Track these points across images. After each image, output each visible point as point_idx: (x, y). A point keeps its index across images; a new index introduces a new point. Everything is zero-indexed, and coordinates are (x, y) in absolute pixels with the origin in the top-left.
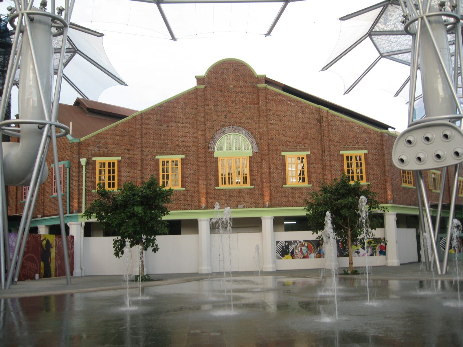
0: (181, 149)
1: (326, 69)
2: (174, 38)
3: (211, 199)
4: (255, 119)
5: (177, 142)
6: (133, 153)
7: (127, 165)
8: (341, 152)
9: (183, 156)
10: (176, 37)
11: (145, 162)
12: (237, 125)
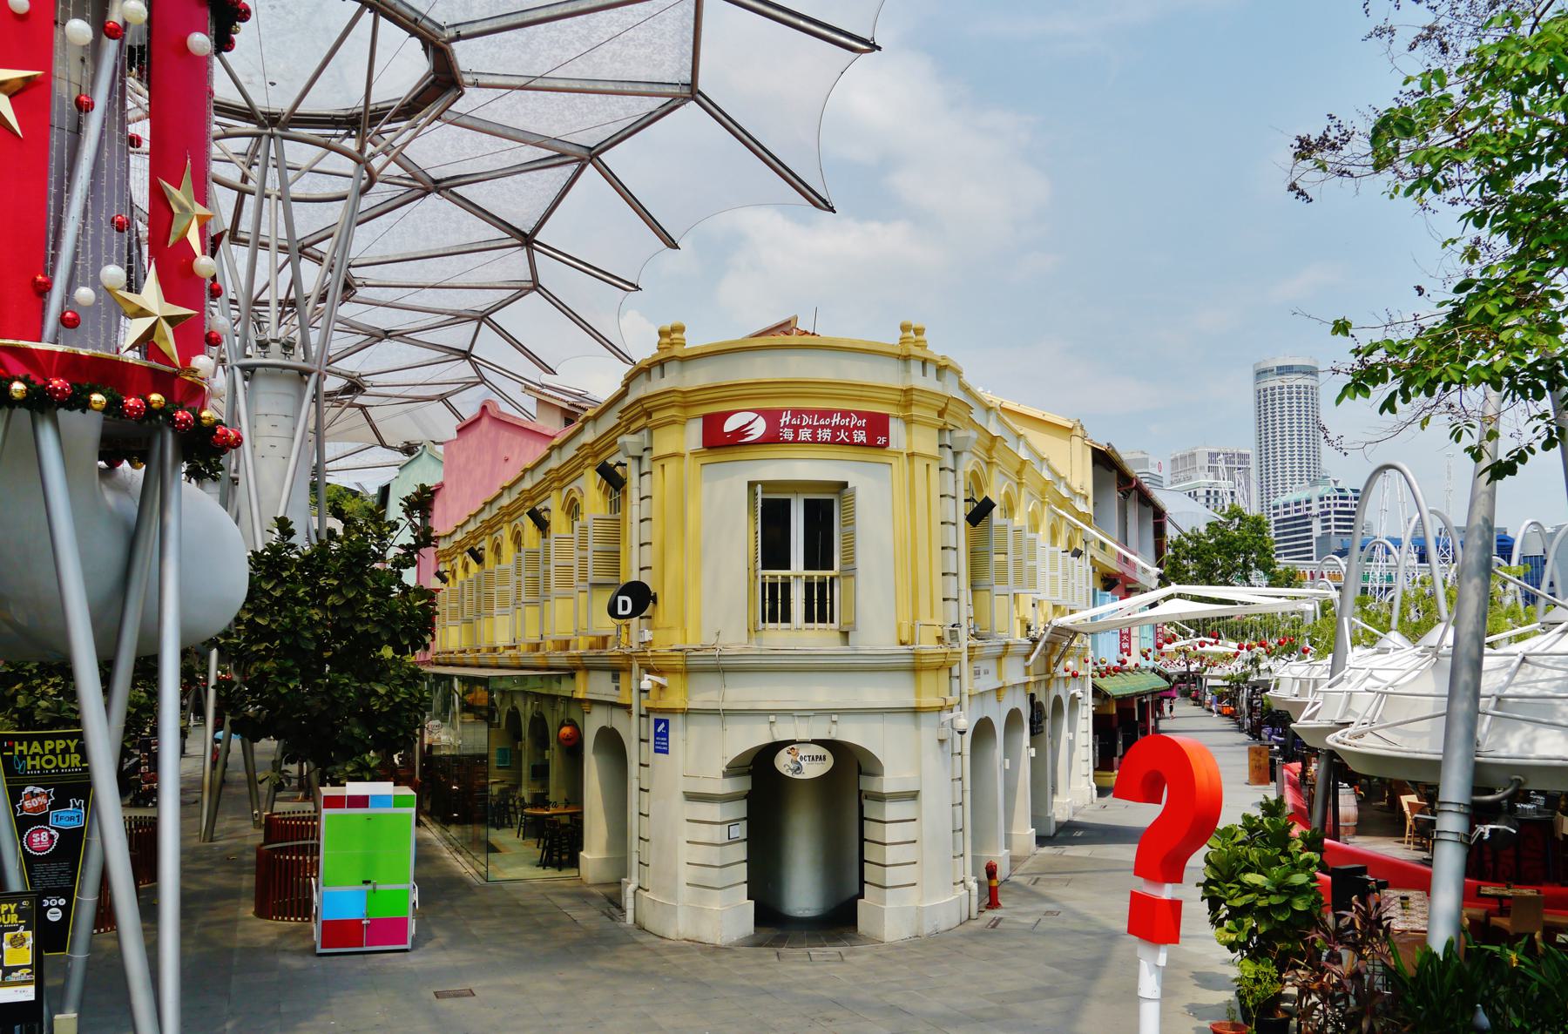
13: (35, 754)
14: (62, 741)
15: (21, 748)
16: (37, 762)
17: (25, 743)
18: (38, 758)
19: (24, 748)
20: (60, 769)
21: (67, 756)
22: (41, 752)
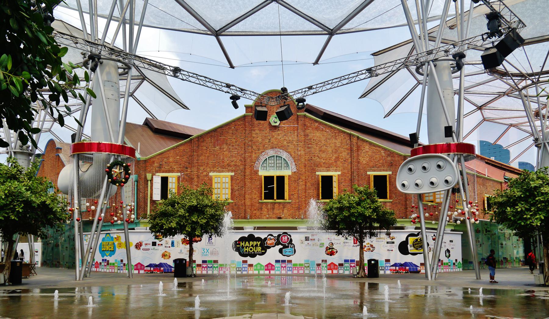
0: (231, 168)
1: (365, 97)
2: (232, 67)
3: (255, 210)
4: (294, 143)
5: (228, 162)
6: (190, 170)
7: (185, 180)
8: (368, 173)
9: (233, 174)
10: (234, 65)
11: (201, 178)
12: (279, 148)
13: (247, 246)
14: (255, 242)
15: (242, 244)
16: (247, 249)
17: (244, 242)
18: (248, 248)
19: (244, 244)
20: (255, 252)
21: (257, 248)
22: (249, 246)
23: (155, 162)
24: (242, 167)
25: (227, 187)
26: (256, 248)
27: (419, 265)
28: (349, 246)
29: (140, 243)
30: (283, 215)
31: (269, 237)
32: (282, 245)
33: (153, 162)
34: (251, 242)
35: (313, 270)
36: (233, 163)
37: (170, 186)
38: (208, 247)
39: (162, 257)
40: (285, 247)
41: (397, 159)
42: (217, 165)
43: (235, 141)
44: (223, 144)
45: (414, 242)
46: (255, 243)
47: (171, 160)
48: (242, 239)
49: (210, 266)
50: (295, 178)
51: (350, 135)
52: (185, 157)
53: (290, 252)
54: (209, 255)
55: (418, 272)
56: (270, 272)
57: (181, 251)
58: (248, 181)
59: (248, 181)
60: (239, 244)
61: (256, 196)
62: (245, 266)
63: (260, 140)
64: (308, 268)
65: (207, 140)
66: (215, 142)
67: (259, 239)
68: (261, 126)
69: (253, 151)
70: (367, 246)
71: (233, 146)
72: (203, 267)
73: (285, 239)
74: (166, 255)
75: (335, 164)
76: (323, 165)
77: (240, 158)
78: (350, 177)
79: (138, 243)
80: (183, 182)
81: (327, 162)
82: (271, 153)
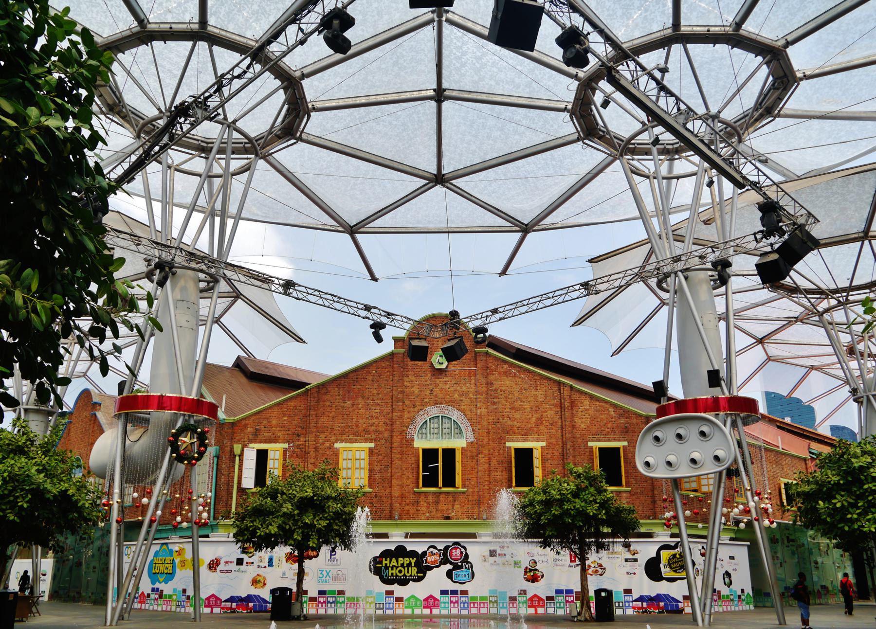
1: (579, 324)
2: (374, 279)
4: (471, 395)
5: (364, 426)
7: (295, 455)
8: (590, 444)
9: (372, 445)
10: (377, 276)
11: (320, 452)
12: (446, 403)
14: (407, 559)
16: (394, 572)
17: (388, 559)
19: (388, 562)
20: (406, 576)
23: (249, 426)
24: (386, 434)
25: (362, 466)
26: (408, 569)
27: (681, 599)
28: (563, 565)
29: (217, 561)
30: (453, 514)
31: (431, 550)
32: (451, 563)
33: (246, 426)
34: (400, 559)
35: (503, 607)
36: (373, 428)
37: (270, 464)
38: (328, 568)
39: (252, 585)
40: (457, 567)
41: (635, 421)
42: (347, 430)
43: (376, 392)
44: (357, 397)
45: (670, 559)
46: (407, 561)
47: (274, 422)
48: (386, 554)
49: (331, 600)
50: (472, 452)
51: (559, 384)
52: (296, 417)
53: (464, 576)
54: (331, 581)
55: (680, 611)
56: (431, 612)
57: (284, 574)
58: (397, 456)
59: (396, 457)
60: (381, 563)
61: (408, 482)
62: (391, 600)
63: (416, 391)
64: (495, 604)
65: (332, 390)
66: (345, 395)
67: (413, 554)
68: (418, 370)
69: (406, 408)
70: (592, 566)
71: (373, 400)
72: (319, 602)
73: (456, 553)
74: (259, 581)
75: (536, 429)
76: (517, 431)
77: (384, 420)
78: (560, 450)
79: (213, 561)
80: (292, 459)
81: (523, 426)
82: (434, 411)
